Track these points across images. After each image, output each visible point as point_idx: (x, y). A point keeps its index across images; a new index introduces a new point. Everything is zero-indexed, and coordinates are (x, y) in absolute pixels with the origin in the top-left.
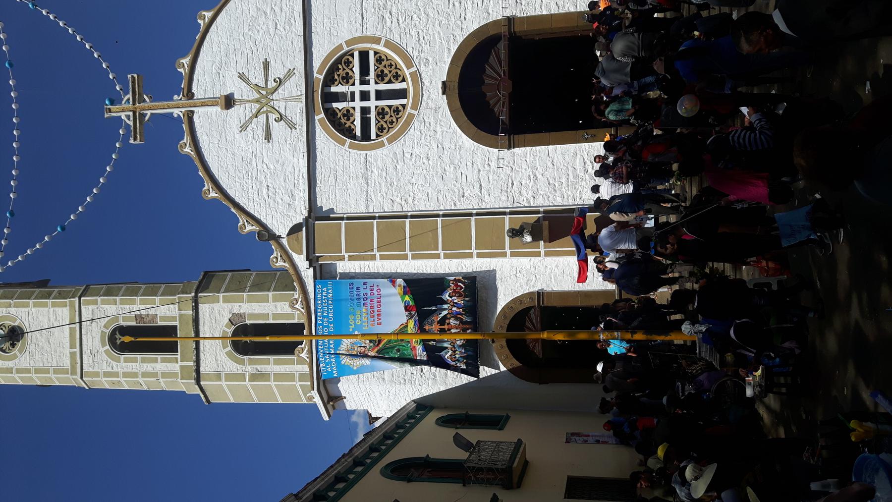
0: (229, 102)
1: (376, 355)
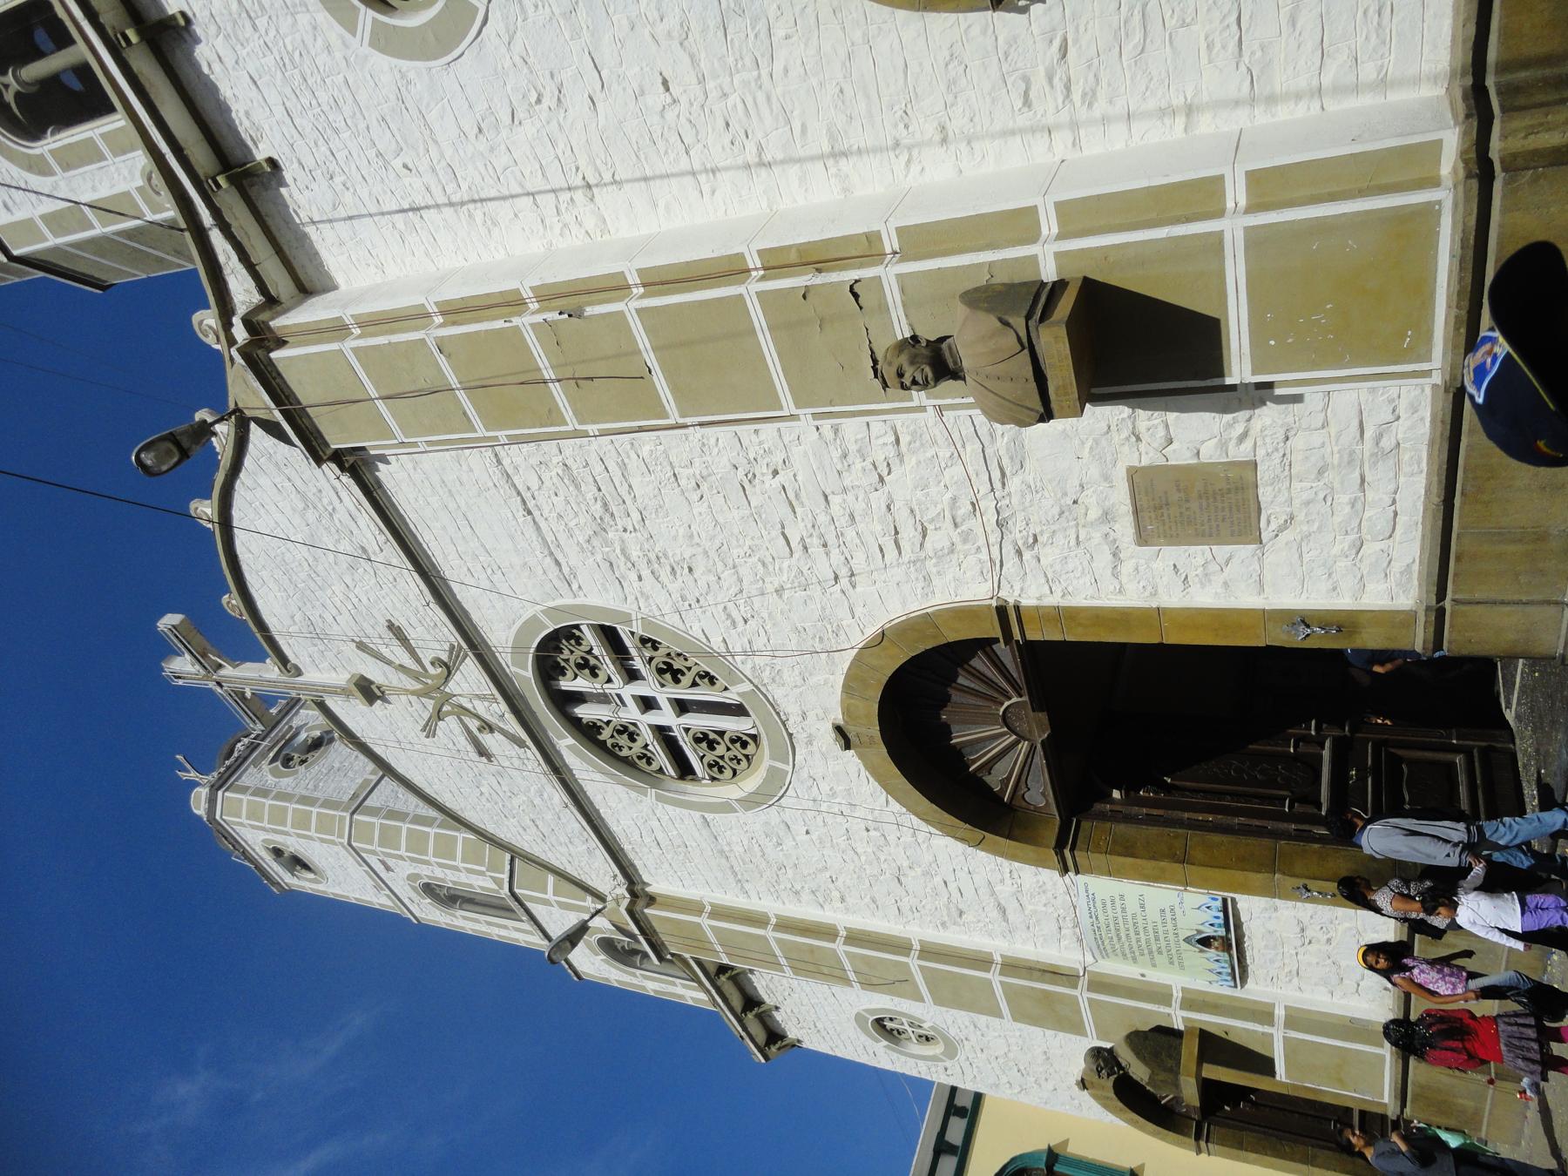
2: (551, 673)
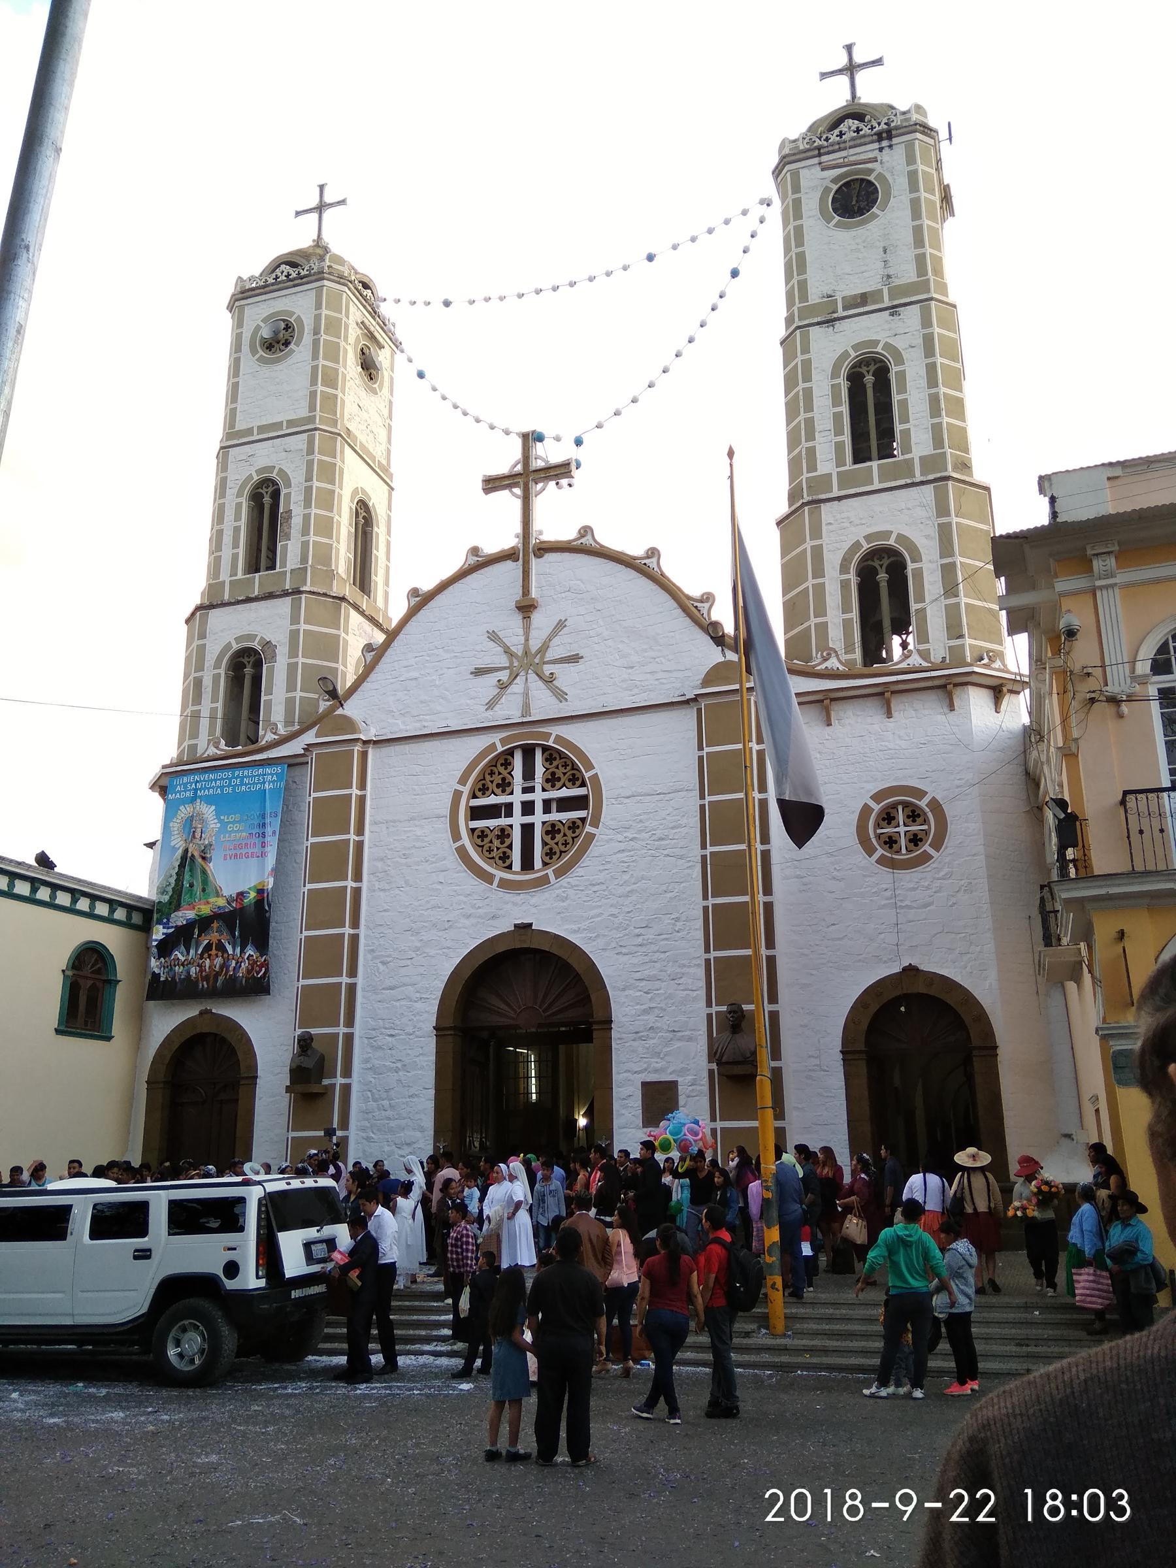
0: (526, 608)
1: (189, 855)
2: (548, 752)
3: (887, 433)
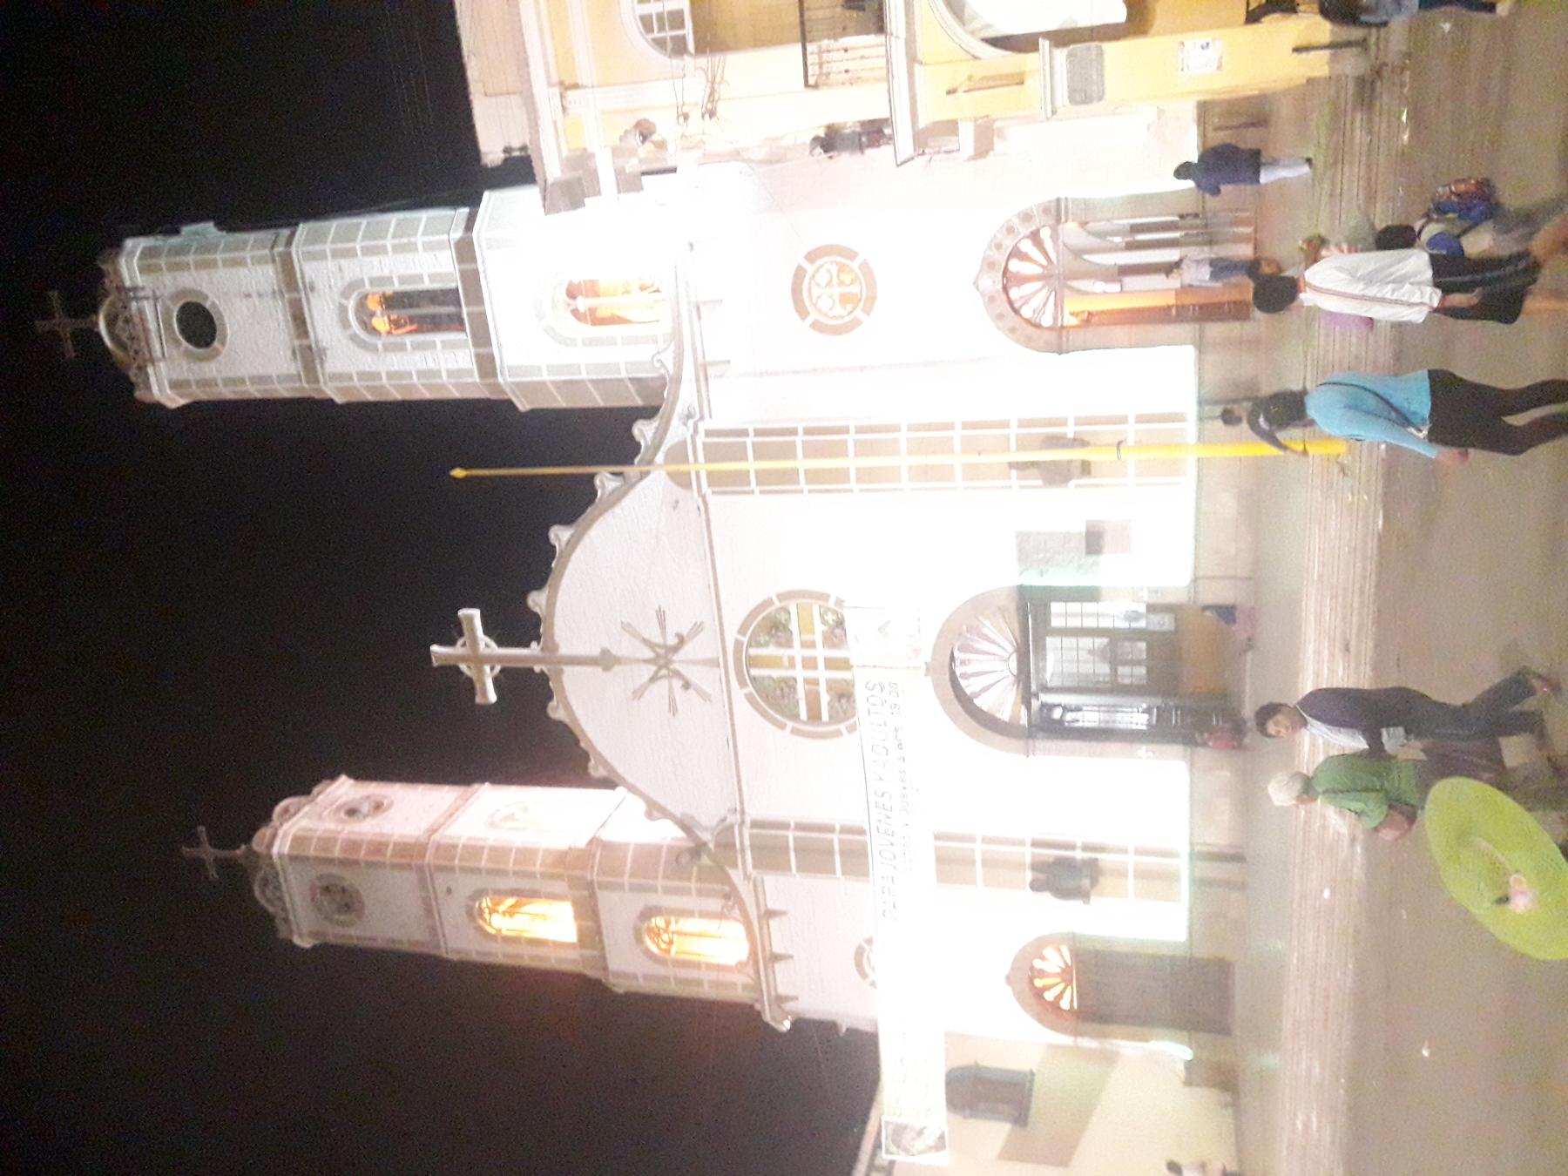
3: (433, 297)
